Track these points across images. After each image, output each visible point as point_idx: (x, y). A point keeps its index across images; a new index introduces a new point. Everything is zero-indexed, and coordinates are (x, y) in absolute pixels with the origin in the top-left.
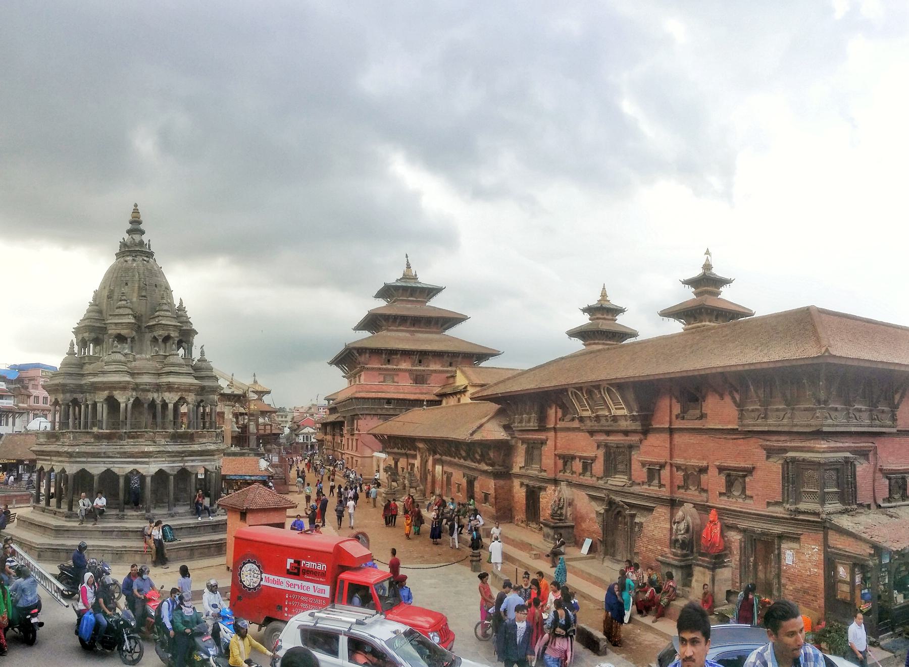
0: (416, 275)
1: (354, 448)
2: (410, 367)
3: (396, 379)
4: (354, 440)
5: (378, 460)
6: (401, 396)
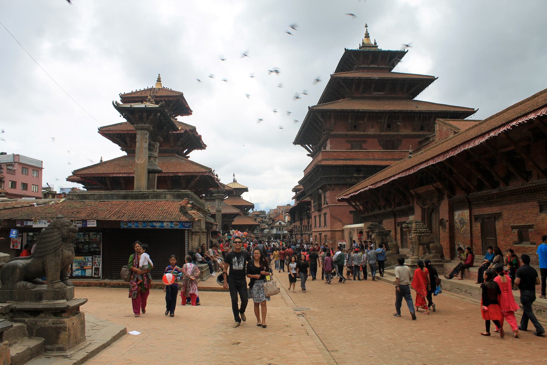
0: (375, 43)
1: (323, 224)
2: (378, 133)
3: (364, 146)
4: (322, 215)
5: (351, 231)
6: (372, 163)
